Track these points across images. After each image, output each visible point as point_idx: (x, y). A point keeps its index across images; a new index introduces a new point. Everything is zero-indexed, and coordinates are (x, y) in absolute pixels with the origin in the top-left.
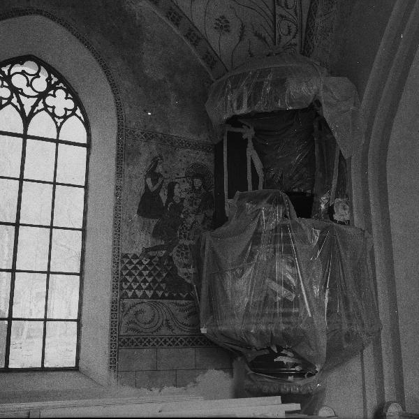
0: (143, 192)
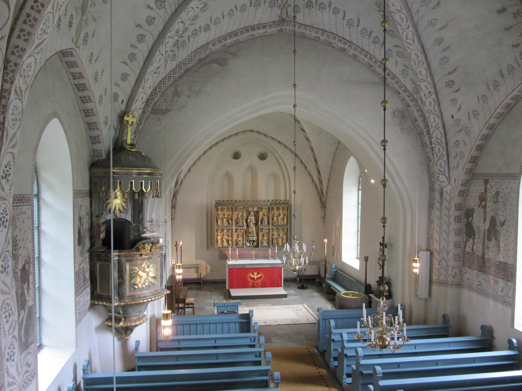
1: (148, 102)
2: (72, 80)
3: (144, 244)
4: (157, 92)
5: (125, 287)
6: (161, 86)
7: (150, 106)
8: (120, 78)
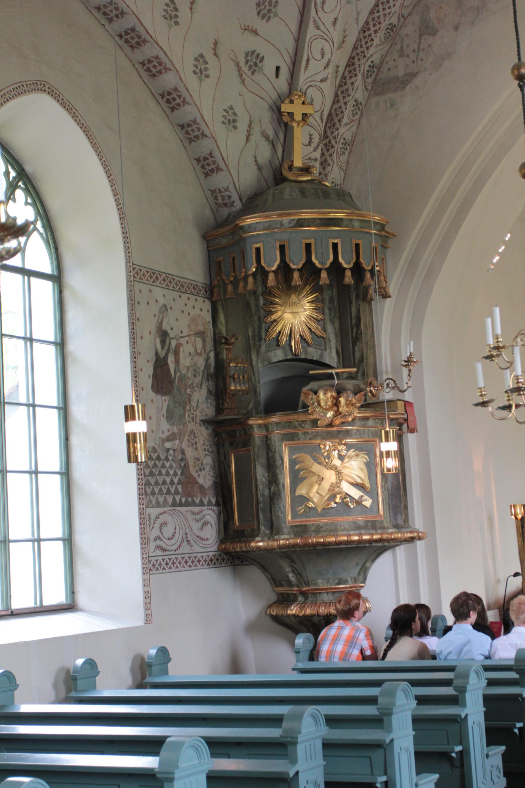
0: (154, 359)
1: (353, 64)
2: (107, 27)
3: (316, 393)
4: (370, 35)
5: (281, 505)
6: (379, 17)
7: (357, 72)
8: (255, 12)
